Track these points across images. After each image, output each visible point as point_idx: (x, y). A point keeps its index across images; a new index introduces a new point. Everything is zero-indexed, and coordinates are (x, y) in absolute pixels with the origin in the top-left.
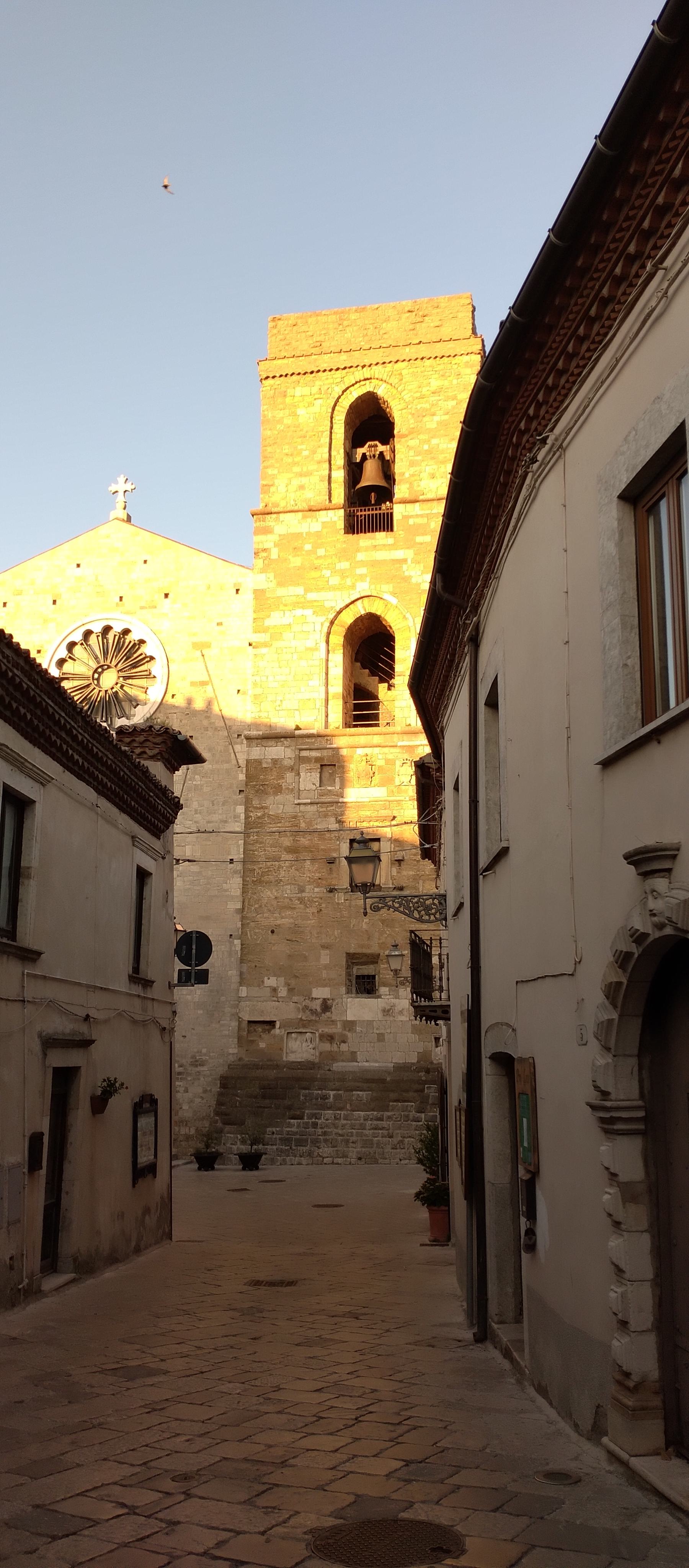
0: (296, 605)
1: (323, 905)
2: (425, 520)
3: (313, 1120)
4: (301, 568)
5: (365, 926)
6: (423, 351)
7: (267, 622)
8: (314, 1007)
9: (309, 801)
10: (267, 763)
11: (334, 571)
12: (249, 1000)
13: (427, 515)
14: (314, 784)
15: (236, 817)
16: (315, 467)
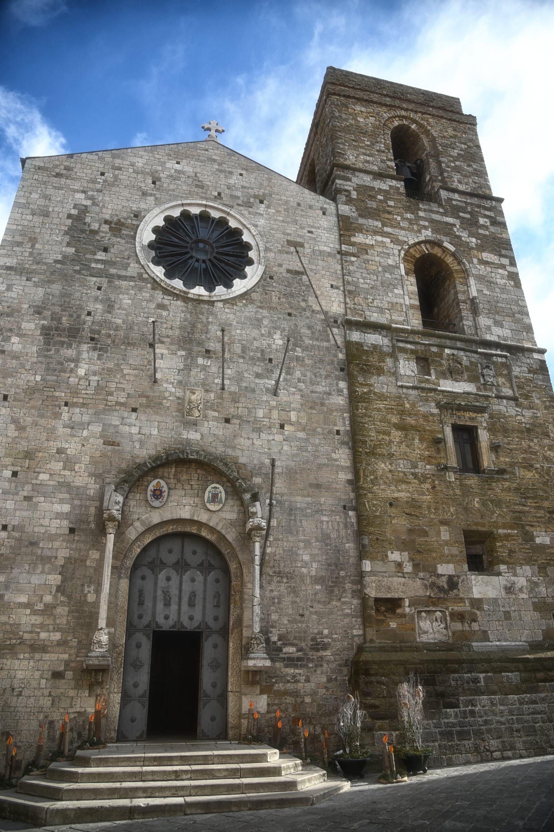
1: (436, 482)
2: (464, 205)
3: (470, 708)
4: (377, 209)
5: (477, 505)
6: (441, 113)
7: (353, 239)
8: (441, 584)
10: (368, 347)
11: (403, 219)
12: (375, 575)
13: (465, 202)
14: (412, 371)
15: (340, 391)
16: (376, 153)
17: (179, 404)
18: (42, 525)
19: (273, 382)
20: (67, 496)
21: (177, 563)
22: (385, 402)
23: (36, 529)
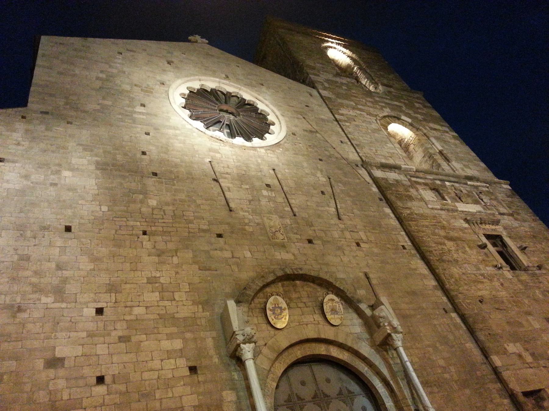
0: (354, 108)
9: (439, 207)
17: (261, 229)
18: (152, 370)
19: (334, 210)
20: (175, 330)
21: (315, 396)
22: (427, 221)
23: (146, 375)
